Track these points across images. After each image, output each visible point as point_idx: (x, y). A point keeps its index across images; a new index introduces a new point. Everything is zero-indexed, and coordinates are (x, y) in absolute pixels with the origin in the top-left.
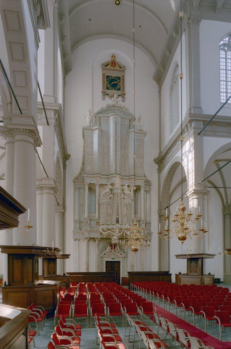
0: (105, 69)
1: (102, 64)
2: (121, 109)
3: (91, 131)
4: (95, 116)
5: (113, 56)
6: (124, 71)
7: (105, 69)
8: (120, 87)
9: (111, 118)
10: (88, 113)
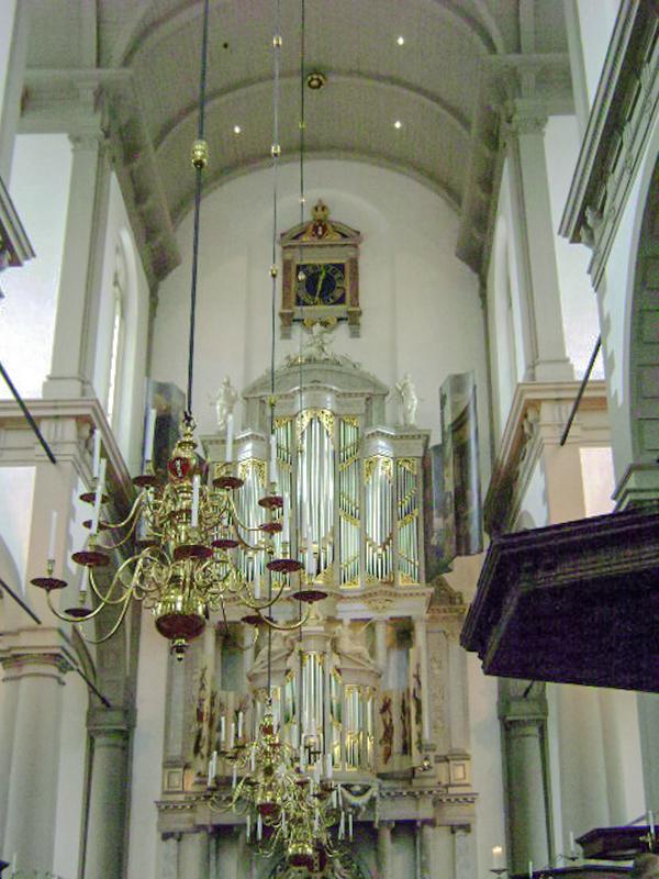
0: (290, 247)
1: (282, 235)
4: (246, 399)
5: (321, 207)
6: (355, 246)
9: (301, 401)
10: (222, 391)
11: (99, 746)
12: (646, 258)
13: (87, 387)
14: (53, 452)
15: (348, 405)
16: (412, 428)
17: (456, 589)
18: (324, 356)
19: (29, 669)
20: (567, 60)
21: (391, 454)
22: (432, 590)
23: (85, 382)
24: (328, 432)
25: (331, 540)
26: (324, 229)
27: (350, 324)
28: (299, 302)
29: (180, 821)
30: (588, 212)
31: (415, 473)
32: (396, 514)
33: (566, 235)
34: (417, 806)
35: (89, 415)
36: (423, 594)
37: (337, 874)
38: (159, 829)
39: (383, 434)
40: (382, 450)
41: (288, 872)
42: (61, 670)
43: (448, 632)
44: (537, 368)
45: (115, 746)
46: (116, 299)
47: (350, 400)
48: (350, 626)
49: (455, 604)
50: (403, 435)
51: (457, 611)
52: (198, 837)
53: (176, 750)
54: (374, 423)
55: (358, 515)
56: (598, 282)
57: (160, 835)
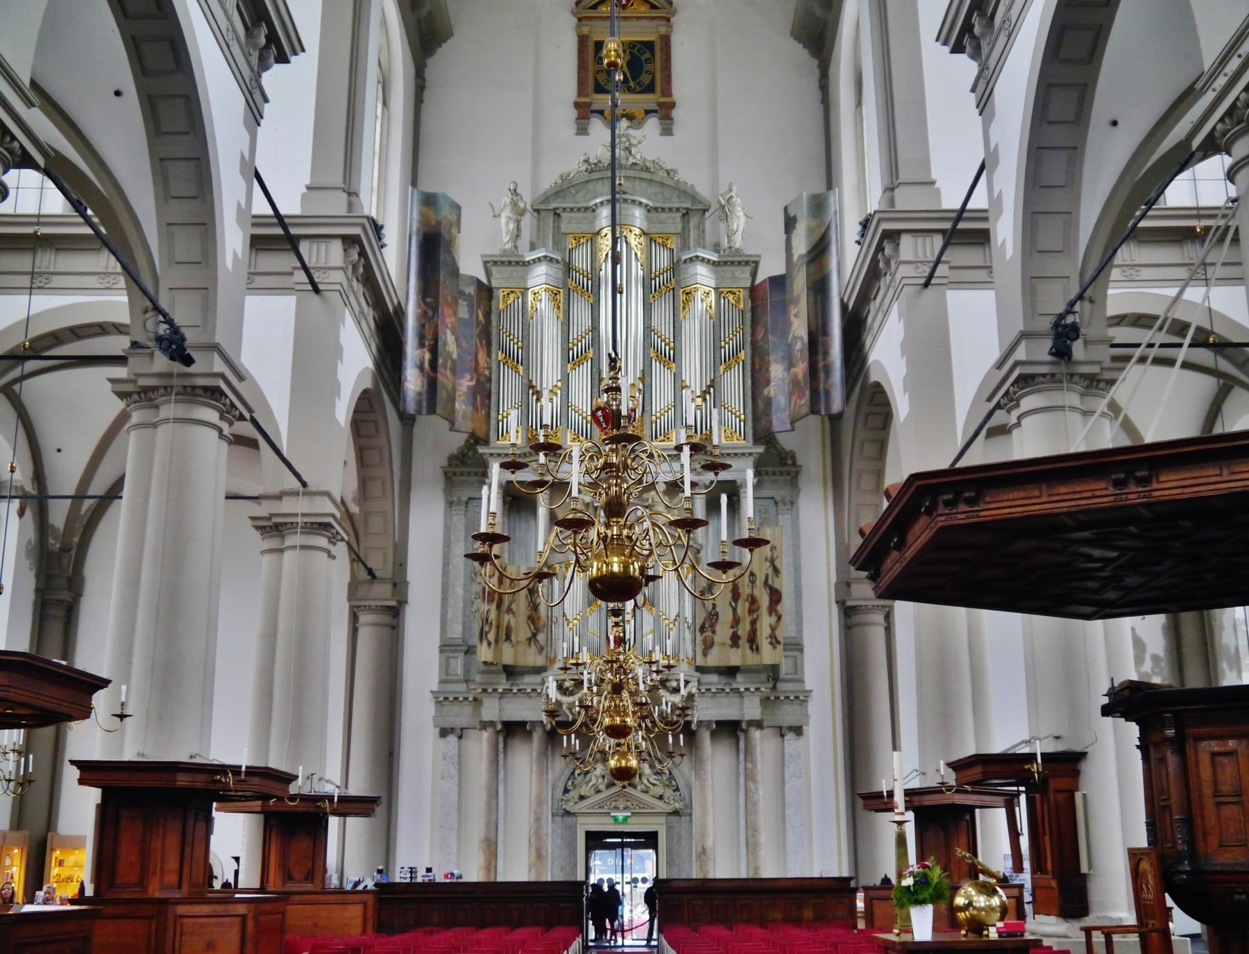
3: (519, 268)
4: (538, 211)
6: (668, 20)
8: (652, 83)
10: (508, 201)
11: (364, 625)
12: (1049, 86)
13: (354, 199)
14: (316, 280)
15: (661, 222)
17: (788, 447)
18: (631, 160)
19: (289, 541)
22: (761, 449)
23: (352, 194)
24: (636, 254)
25: (641, 386)
27: (660, 119)
28: (599, 89)
29: (461, 716)
30: (975, 18)
31: (741, 306)
32: (719, 359)
33: (945, 43)
34: (741, 704)
35: (358, 236)
36: (751, 454)
37: (645, 781)
38: (435, 726)
39: (703, 259)
40: (703, 278)
41: (588, 777)
42: (330, 542)
43: (778, 499)
44: (897, 191)
45: (385, 625)
46: (379, 82)
47: (663, 216)
48: (665, 493)
49: (785, 464)
50: (727, 262)
51: (788, 474)
52: (486, 735)
53: (456, 631)
54: (692, 244)
55: (672, 358)
56: (984, 103)
57: (438, 730)
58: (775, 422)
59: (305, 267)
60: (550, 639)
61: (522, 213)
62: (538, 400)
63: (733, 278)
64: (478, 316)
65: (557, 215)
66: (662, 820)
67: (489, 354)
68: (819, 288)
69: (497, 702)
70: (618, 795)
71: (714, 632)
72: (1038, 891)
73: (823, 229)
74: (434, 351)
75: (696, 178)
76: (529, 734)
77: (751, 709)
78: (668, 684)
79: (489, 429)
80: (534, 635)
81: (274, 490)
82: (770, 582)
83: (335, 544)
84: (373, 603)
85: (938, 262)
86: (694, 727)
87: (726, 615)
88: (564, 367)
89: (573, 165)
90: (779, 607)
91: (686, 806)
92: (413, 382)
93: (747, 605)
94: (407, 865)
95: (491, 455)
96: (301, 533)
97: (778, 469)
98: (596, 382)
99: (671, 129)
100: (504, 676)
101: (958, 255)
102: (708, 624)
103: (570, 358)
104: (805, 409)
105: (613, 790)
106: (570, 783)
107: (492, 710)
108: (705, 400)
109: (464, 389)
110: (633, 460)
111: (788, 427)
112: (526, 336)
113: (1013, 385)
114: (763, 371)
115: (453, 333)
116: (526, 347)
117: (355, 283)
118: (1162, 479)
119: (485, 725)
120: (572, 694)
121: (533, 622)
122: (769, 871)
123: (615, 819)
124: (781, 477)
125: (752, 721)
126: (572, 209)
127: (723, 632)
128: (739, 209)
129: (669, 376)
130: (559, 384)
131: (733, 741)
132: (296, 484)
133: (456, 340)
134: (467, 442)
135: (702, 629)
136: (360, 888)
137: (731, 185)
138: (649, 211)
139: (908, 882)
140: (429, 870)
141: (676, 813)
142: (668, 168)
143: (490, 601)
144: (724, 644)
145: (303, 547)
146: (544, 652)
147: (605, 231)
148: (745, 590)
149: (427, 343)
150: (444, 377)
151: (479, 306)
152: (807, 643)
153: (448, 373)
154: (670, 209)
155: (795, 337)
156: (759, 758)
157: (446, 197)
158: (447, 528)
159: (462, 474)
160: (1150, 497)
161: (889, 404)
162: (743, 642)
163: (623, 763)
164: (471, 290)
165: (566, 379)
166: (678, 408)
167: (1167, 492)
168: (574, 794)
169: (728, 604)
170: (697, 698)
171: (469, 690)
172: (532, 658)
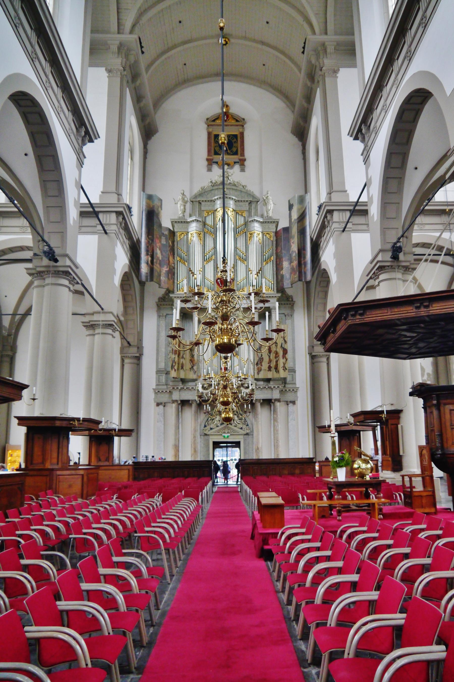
0: (211, 125)
1: (207, 119)
2: (234, 187)
3: (186, 224)
4: (192, 202)
6: (243, 126)
7: (211, 125)
10: (181, 197)
12: (391, 153)
15: (241, 206)
16: (271, 218)
17: (290, 294)
18: (229, 182)
19: (98, 331)
20: (354, 39)
21: (261, 230)
22: (279, 295)
25: (233, 270)
26: (227, 117)
27: (240, 165)
28: (216, 153)
29: (164, 398)
30: (363, 126)
32: (264, 260)
33: (351, 136)
34: (272, 393)
36: (275, 297)
37: (235, 422)
38: (155, 402)
39: (257, 221)
40: (257, 228)
41: (214, 421)
42: (113, 331)
43: (286, 314)
44: (332, 194)
47: (241, 203)
51: (290, 304)
52: (174, 405)
54: (252, 215)
55: (245, 259)
56: (366, 160)
57: (156, 403)
58: (285, 284)
59: (101, 224)
60: (198, 368)
61: (186, 202)
62: (193, 276)
63: (269, 228)
64: (169, 243)
65: (200, 203)
66: (242, 437)
67: (174, 258)
68: (302, 232)
69: (178, 392)
70: (225, 428)
71: (261, 365)
72: (384, 462)
73: (304, 209)
74: (152, 257)
75: (254, 188)
76: (191, 405)
77: (276, 395)
78: (244, 385)
79: (174, 287)
80: (192, 367)
81: (91, 312)
82: (283, 346)
83: (115, 332)
84: (130, 355)
85: (348, 222)
86: (254, 402)
87: (266, 359)
88: (203, 263)
89: (206, 184)
90: (286, 356)
91: (251, 432)
92: (144, 269)
93: (274, 355)
94: (145, 455)
95: (175, 297)
96: (102, 328)
97: (286, 302)
98: (216, 268)
99: (244, 169)
100: (181, 382)
101: (356, 219)
102: (259, 362)
103: (205, 260)
104: (297, 279)
105: (223, 426)
106: (207, 423)
107: (176, 396)
108: (258, 276)
109: (164, 271)
110: (232, 299)
111: (290, 286)
112: (188, 251)
113: (376, 270)
114: (280, 264)
115: (160, 249)
116: (188, 255)
117: (121, 230)
118: (434, 306)
119: (174, 402)
120: (207, 389)
121: (192, 362)
122: (283, 455)
123: (224, 437)
124: (287, 306)
125: (276, 399)
126: (206, 201)
127: (265, 365)
128: (271, 201)
129: (244, 266)
130: (201, 270)
131: (269, 407)
132: (99, 309)
133: (161, 252)
134: (166, 292)
135: (257, 364)
136: (127, 464)
137: (268, 192)
138: (236, 202)
139: (336, 459)
140: (153, 457)
141: (247, 434)
142: (243, 184)
143: (175, 354)
144: (265, 370)
145: (102, 333)
146: (196, 373)
147: (219, 210)
148: (273, 349)
149: (149, 254)
150: (156, 267)
151: (169, 239)
152: (297, 369)
153: (158, 265)
154: (244, 201)
155: (292, 251)
156: (279, 413)
157: (156, 196)
158: (158, 326)
159: (164, 305)
160: (429, 313)
161: (329, 277)
162: (273, 369)
163: (227, 415)
164: (166, 233)
165: (204, 268)
166: (248, 279)
167: (435, 311)
168: (208, 427)
169: (267, 355)
170: (255, 390)
171: (167, 388)
172: (192, 376)
